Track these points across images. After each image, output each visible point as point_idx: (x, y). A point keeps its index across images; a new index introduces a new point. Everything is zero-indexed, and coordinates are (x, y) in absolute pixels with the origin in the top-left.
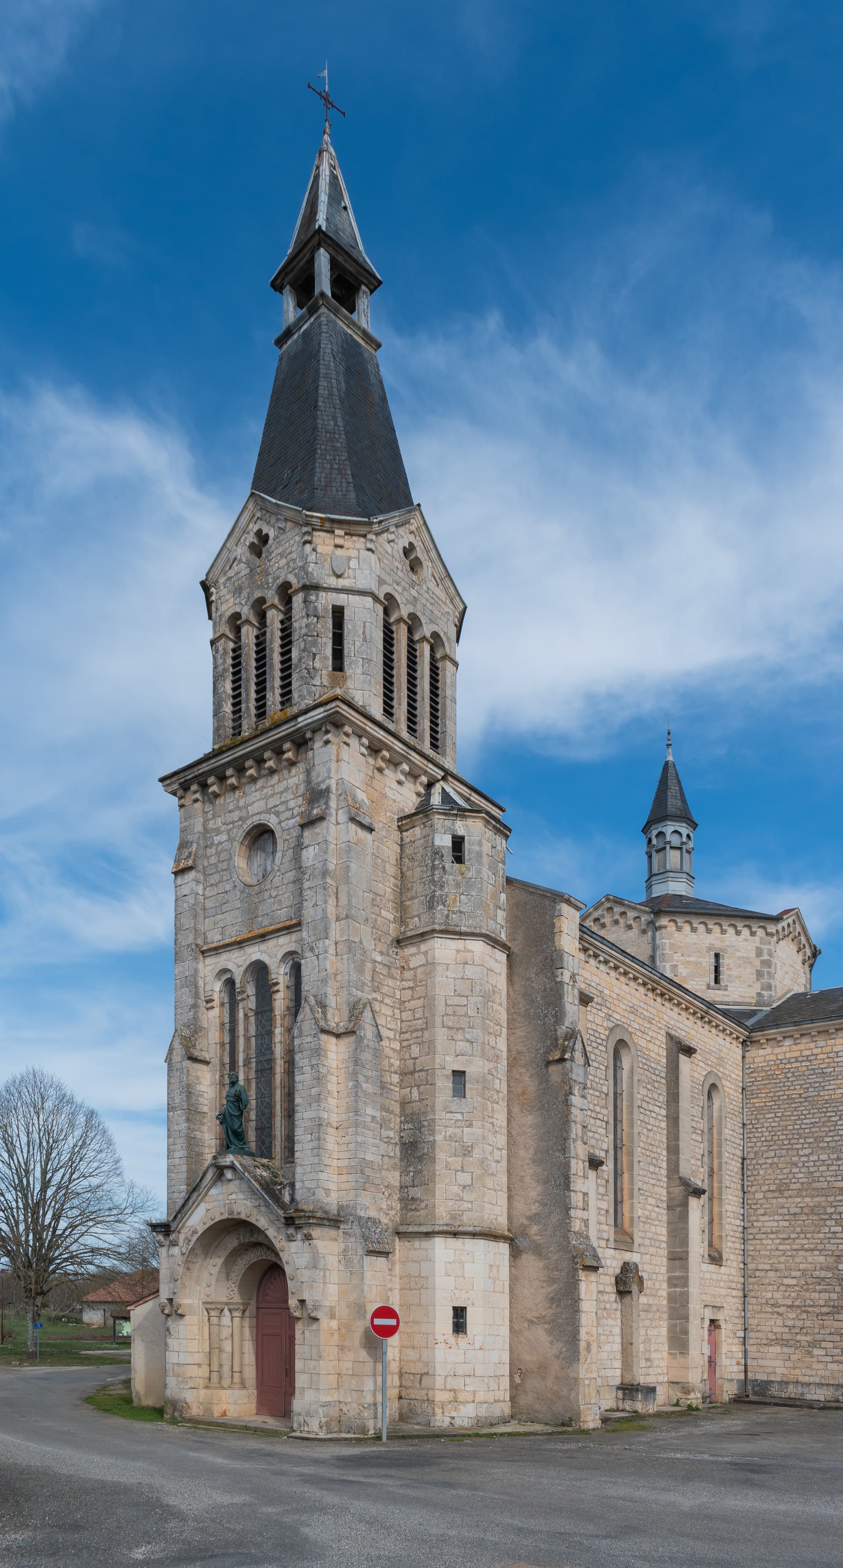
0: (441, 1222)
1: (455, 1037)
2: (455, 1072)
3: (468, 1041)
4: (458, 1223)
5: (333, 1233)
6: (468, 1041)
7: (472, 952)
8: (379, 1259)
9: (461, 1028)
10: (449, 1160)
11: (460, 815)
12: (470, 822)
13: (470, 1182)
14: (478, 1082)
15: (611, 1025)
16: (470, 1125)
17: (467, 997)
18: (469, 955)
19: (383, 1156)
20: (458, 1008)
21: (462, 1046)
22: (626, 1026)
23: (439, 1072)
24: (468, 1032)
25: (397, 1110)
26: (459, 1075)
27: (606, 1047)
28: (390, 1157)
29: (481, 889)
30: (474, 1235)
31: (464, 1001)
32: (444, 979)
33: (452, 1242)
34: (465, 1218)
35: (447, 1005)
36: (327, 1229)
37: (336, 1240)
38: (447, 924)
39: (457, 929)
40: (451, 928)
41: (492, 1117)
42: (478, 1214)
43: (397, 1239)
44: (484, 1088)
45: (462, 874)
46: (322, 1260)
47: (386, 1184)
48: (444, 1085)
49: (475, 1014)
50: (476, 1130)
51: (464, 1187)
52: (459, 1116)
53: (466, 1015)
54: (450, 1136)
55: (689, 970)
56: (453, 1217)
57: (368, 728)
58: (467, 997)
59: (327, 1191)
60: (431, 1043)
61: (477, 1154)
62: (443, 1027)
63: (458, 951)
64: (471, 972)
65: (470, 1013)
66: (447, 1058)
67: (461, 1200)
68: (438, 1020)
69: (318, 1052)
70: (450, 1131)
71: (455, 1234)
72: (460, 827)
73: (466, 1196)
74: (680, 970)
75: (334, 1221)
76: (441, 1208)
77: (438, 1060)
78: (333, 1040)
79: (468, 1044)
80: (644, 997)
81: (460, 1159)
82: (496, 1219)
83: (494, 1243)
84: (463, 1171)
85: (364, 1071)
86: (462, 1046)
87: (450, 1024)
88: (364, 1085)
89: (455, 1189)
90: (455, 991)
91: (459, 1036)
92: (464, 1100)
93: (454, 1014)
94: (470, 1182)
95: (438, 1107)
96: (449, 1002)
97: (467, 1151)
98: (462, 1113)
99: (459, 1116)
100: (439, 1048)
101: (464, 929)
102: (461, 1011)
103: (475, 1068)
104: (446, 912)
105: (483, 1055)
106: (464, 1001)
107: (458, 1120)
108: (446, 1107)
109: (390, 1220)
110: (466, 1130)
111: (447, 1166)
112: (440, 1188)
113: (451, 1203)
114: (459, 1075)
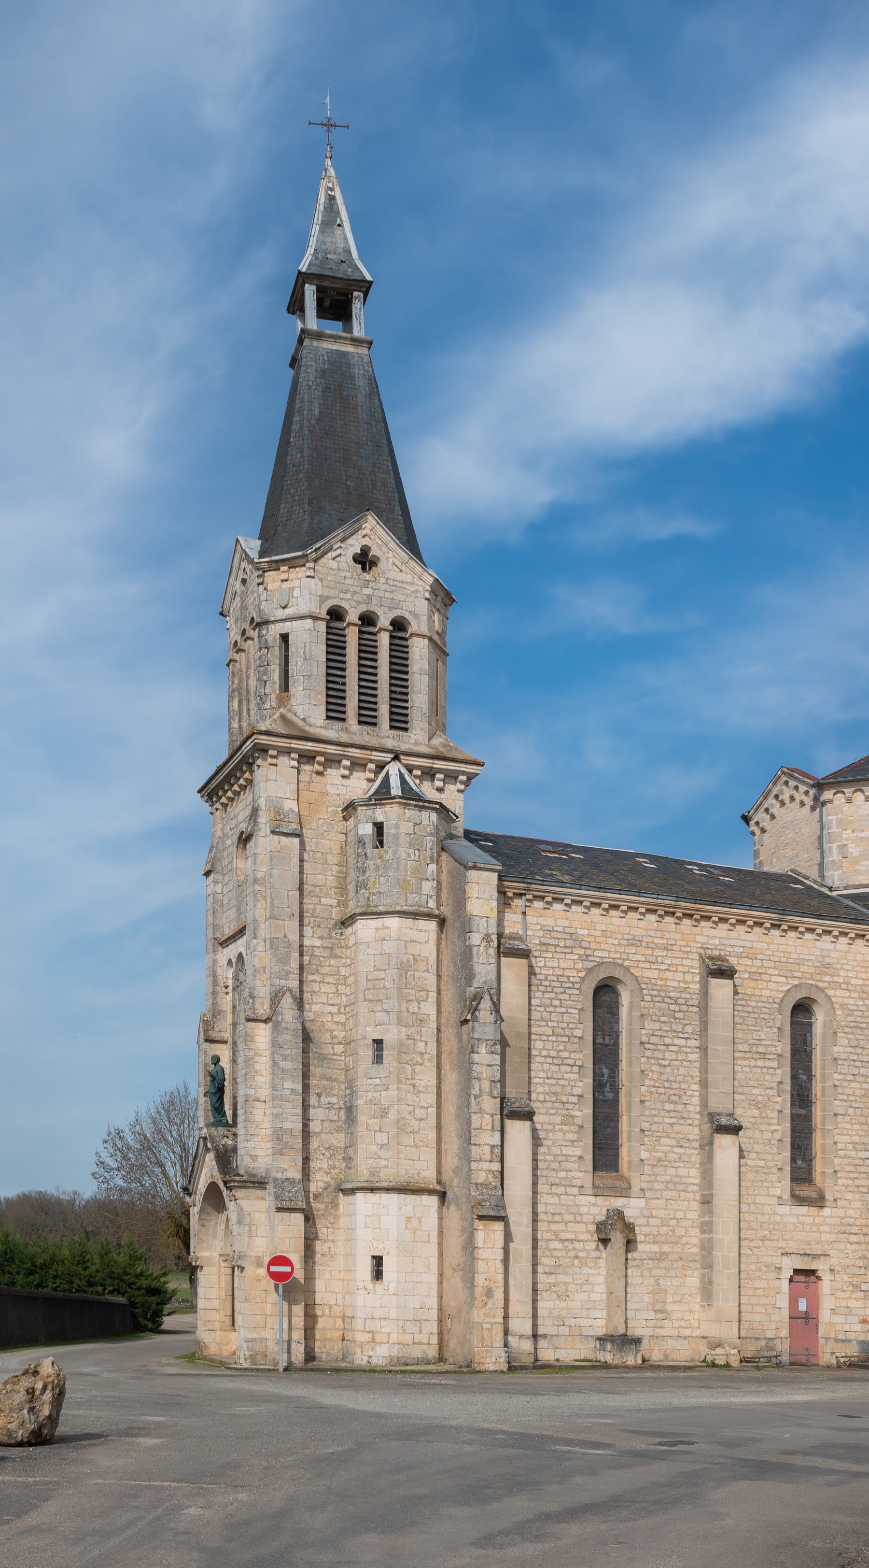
0: (363, 1179)
1: (375, 1009)
2: (374, 1041)
3: (385, 1011)
4: (377, 1179)
5: (260, 1193)
6: (385, 1011)
7: (389, 928)
8: (293, 1214)
9: (379, 1000)
10: (369, 1121)
11: (379, 804)
12: (388, 808)
13: (386, 1142)
14: (393, 1048)
15: (589, 965)
16: (387, 1089)
17: (385, 970)
18: (387, 931)
19: (323, 1121)
20: (377, 982)
21: (380, 1016)
22: (620, 962)
23: (361, 1042)
24: (386, 1003)
25: (342, 1078)
26: (378, 1043)
27: (579, 989)
28: (332, 1121)
29: (398, 869)
30: (388, 1190)
31: (382, 975)
32: (366, 956)
33: (370, 1196)
34: (382, 1175)
35: (368, 980)
36: (252, 1190)
37: (263, 1199)
38: (368, 906)
39: (374, 910)
40: (369, 910)
41: (413, 1079)
42: (393, 1170)
43: (341, 1195)
44: (400, 1053)
45: (381, 857)
46: (247, 1217)
47: (327, 1146)
48: (366, 1053)
49: (392, 986)
50: (393, 1093)
51: (382, 1146)
52: (377, 1081)
53: (384, 987)
54: (370, 1100)
55: (861, 849)
56: (372, 1174)
57: (293, 745)
58: (385, 970)
59: (254, 1158)
60: (355, 1016)
61: (393, 1115)
62: (365, 1000)
63: (377, 929)
64: (389, 947)
65: (387, 985)
66: (368, 1029)
67: (379, 1158)
68: (361, 995)
69: (249, 1038)
70: (370, 1095)
71: (372, 1190)
72: (379, 814)
73: (384, 1154)
74: (851, 850)
75: (260, 1184)
76: (363, 1166)
77: (360, 1031)
78: (263, 1025)
79: (385, 1014)
80: (655, 924)
81: (378, 1120)
82: (419, 1174)
83: (414, 1197)
84: (380, 1131)
85: (282, 1051)
86: (380, 1016)
87: (371, 997)
88: (282, 1064)
89: (374, 1148)
90: (375, 966)
91: (378, 1008)
92: (381, 1066)
93: (374, 988)
94: (386, 1142)
95: (360, 1074)
96: (370, 977)
97: (384, 1113)
98: (380, 1078)
99: (377, 1081)
100: (361, 1020)
101: (381, 909)
102: (380, 984)
103: (390, 1036)
104: (367, 895)
105: (399, 1022)
106: (382, 975)
107: (377, 1085)
108: (367, 1074)
109: (331, 1178)
110: (384, 1093)
111: (368, 1129)
112: (361, 1147)
113: (370, 1161)
114: (378, 1043)
